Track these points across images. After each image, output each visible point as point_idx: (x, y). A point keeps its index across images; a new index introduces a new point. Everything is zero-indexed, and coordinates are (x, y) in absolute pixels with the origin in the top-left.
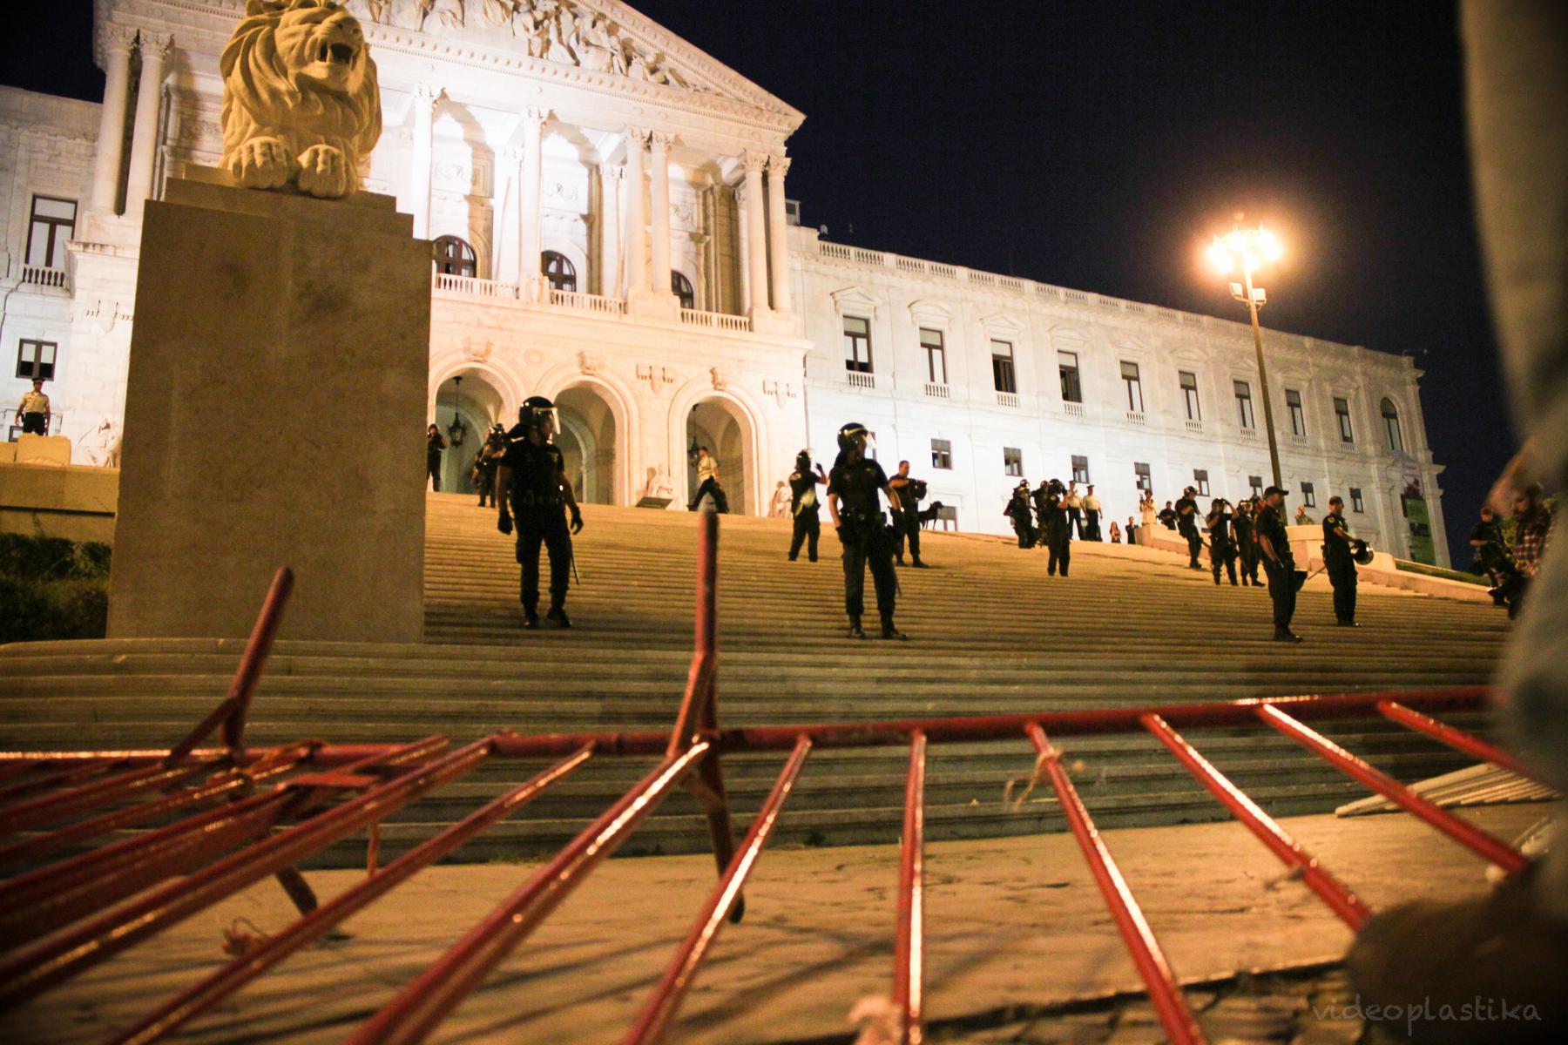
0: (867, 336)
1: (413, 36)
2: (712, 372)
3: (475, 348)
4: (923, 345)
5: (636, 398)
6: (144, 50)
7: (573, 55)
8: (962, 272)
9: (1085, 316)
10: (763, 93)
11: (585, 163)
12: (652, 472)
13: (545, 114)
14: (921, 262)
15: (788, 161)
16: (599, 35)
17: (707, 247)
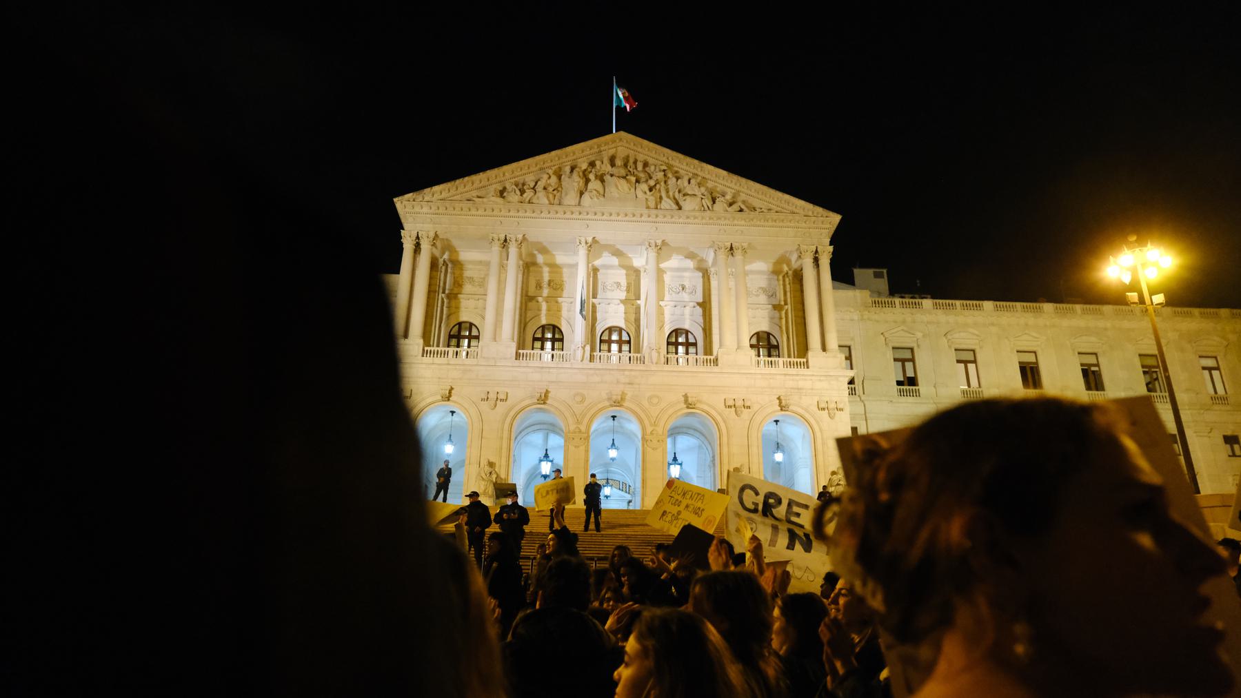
0: (913, 360)
1: (573, 209)
4: (958, 361)
6: (422, 242)
7: (677, 204)
8: (988, 305)
9: (1101, 324)
10: (810, 206)
11: (699, 269)
13: (659, 242)
15: (831, 248)
16: (691, 188)
17: (786, 313)
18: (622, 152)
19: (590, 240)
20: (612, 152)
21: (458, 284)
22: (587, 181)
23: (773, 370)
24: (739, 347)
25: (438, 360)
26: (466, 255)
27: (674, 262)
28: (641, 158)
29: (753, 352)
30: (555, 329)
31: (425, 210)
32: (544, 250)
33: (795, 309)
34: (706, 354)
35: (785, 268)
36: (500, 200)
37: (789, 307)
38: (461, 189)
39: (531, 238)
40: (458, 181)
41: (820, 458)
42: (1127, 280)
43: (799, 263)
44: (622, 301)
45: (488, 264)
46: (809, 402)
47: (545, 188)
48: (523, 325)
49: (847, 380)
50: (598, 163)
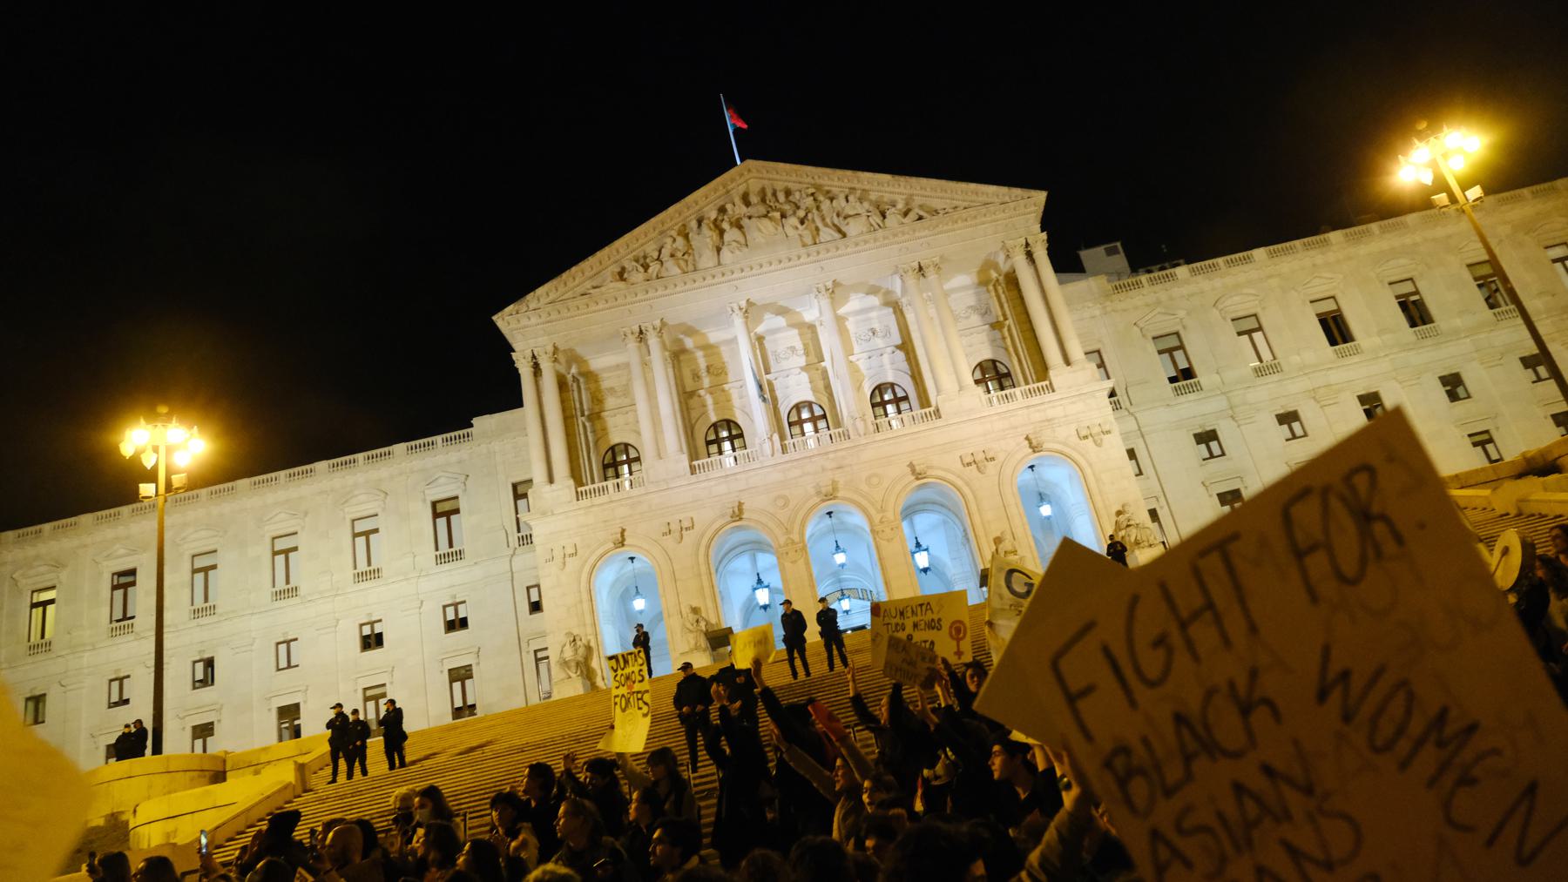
0: (1181, 347)
2: (1027, 438)
3: (824, 490)
4: (1239, 334)
5: (967, 484)
7: (840, 231)
8: (1259, 253)
9: (1408, 240)
10: (1004, 190)
11: (887, 304)
12: (998, 541)
13: (829, 284)
14: (1214, 261)
15: (1044, 236)
18: (754, 186)
19: (743, 304)
20: (742, 189)
21: (597, 399)
22: (722, 232)
23: (1011, 406)
24: (961, 388)
25: (598, 500)
26: (597, 363)
27: (855, 303)
28: (780, 186)
29: (980, 389)
30: (729, 424)
31: (534, 320)
32: (691, 331)
33: (1019, 322)
34: (922, 407)
35: (994, 275)
36: (621, 285)
37: (1010, 321)
38: (571, 284)
39: (671, 323)
40: (564, 275)
41: (1097, 498)
42: (1428, 179)
43: (1009, 263)
44: (803, 369)
45: (627, 365)
46: (1066, 432)
47: (672, 256)
48: (689, 430)
49: (1106, 393)
50: (729, 207)
